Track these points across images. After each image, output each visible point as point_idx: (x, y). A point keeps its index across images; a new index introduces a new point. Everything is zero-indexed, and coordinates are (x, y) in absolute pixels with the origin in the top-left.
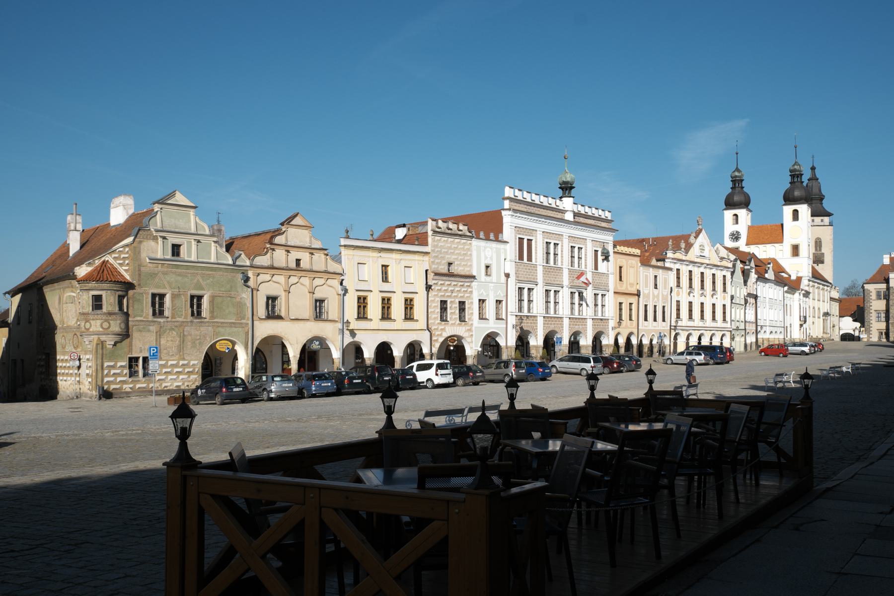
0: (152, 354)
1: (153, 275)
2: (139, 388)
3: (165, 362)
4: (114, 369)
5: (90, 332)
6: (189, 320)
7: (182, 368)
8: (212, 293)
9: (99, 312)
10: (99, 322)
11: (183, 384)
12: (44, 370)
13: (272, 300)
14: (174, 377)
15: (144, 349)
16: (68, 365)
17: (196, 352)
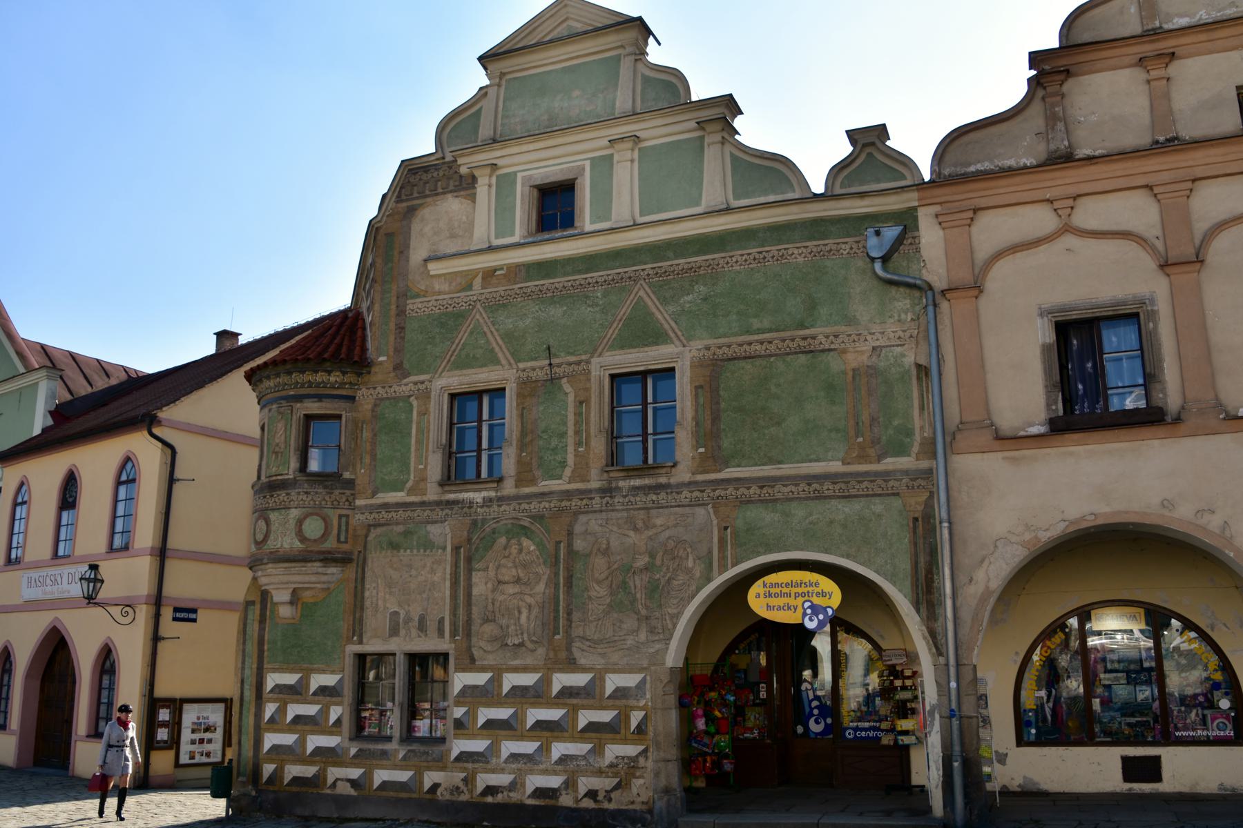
1: (451, 320)
2: (385, 785)
4: (298, 702)
6: (595, 484)
7: (563, 705)
8: (708, 348)
11: (570, 784)
14: (529, 747)
15: (408, 620)
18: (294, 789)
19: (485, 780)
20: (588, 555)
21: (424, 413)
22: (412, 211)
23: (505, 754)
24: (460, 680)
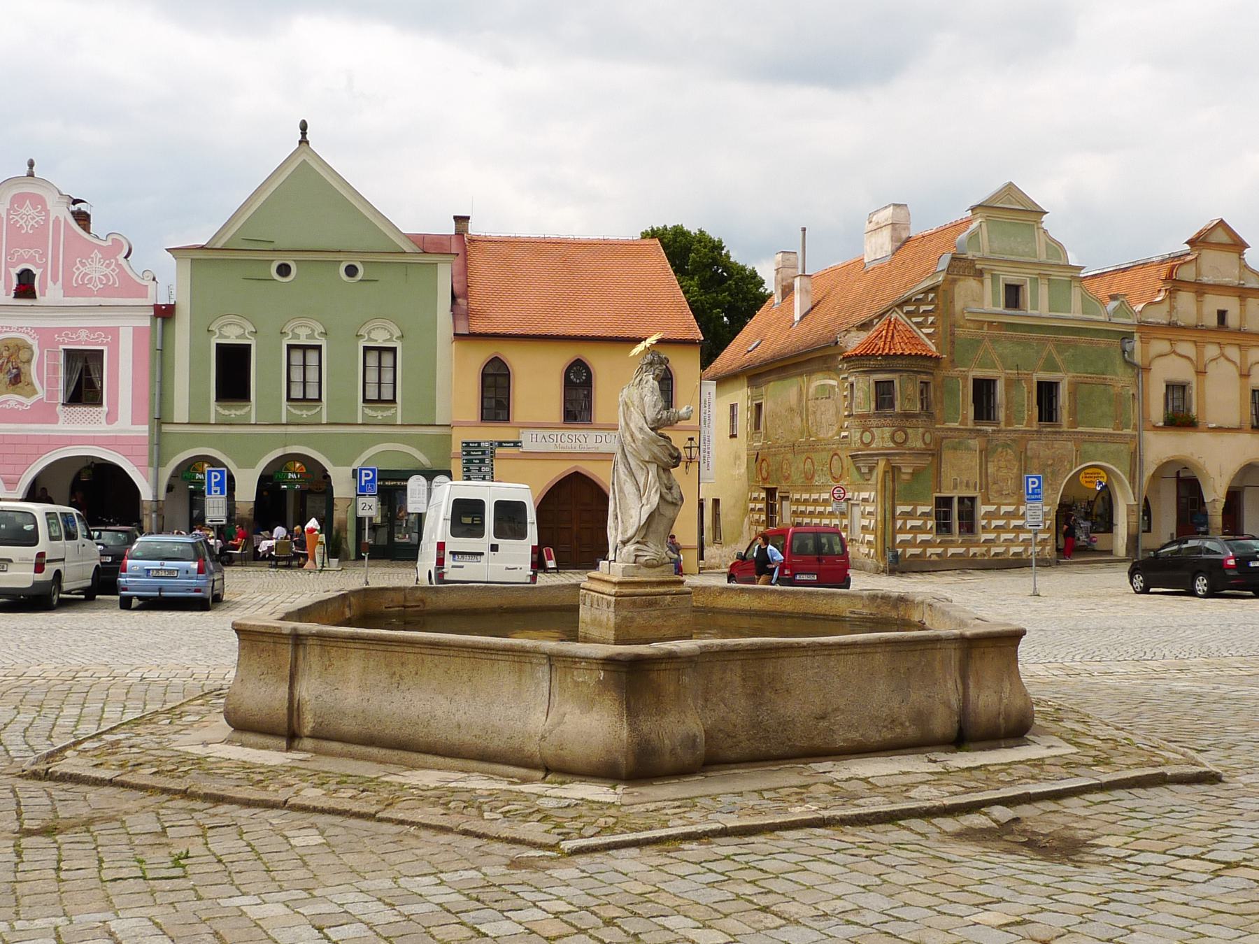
0: (1030, 492)
1: (975, 343)
2: (953, 555)
3: (995, 507)
5: (873, 449)
6: (1035, 428)
9: (889, 411)
10: (887, 432)
11: (1026, 550)
12: (763, 517)
13: (1176, 389)
15: (961, 483)
16: (829, 509)
17: (1047, 490)
18: (911, 559)
19: (994, 550)
20: (1032, 458)
21: (964, 386)
22: (954, 281)
23: (1002, 539)
24: (982, 509)
